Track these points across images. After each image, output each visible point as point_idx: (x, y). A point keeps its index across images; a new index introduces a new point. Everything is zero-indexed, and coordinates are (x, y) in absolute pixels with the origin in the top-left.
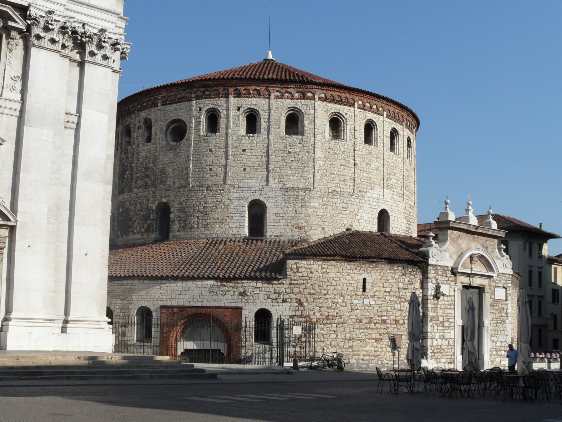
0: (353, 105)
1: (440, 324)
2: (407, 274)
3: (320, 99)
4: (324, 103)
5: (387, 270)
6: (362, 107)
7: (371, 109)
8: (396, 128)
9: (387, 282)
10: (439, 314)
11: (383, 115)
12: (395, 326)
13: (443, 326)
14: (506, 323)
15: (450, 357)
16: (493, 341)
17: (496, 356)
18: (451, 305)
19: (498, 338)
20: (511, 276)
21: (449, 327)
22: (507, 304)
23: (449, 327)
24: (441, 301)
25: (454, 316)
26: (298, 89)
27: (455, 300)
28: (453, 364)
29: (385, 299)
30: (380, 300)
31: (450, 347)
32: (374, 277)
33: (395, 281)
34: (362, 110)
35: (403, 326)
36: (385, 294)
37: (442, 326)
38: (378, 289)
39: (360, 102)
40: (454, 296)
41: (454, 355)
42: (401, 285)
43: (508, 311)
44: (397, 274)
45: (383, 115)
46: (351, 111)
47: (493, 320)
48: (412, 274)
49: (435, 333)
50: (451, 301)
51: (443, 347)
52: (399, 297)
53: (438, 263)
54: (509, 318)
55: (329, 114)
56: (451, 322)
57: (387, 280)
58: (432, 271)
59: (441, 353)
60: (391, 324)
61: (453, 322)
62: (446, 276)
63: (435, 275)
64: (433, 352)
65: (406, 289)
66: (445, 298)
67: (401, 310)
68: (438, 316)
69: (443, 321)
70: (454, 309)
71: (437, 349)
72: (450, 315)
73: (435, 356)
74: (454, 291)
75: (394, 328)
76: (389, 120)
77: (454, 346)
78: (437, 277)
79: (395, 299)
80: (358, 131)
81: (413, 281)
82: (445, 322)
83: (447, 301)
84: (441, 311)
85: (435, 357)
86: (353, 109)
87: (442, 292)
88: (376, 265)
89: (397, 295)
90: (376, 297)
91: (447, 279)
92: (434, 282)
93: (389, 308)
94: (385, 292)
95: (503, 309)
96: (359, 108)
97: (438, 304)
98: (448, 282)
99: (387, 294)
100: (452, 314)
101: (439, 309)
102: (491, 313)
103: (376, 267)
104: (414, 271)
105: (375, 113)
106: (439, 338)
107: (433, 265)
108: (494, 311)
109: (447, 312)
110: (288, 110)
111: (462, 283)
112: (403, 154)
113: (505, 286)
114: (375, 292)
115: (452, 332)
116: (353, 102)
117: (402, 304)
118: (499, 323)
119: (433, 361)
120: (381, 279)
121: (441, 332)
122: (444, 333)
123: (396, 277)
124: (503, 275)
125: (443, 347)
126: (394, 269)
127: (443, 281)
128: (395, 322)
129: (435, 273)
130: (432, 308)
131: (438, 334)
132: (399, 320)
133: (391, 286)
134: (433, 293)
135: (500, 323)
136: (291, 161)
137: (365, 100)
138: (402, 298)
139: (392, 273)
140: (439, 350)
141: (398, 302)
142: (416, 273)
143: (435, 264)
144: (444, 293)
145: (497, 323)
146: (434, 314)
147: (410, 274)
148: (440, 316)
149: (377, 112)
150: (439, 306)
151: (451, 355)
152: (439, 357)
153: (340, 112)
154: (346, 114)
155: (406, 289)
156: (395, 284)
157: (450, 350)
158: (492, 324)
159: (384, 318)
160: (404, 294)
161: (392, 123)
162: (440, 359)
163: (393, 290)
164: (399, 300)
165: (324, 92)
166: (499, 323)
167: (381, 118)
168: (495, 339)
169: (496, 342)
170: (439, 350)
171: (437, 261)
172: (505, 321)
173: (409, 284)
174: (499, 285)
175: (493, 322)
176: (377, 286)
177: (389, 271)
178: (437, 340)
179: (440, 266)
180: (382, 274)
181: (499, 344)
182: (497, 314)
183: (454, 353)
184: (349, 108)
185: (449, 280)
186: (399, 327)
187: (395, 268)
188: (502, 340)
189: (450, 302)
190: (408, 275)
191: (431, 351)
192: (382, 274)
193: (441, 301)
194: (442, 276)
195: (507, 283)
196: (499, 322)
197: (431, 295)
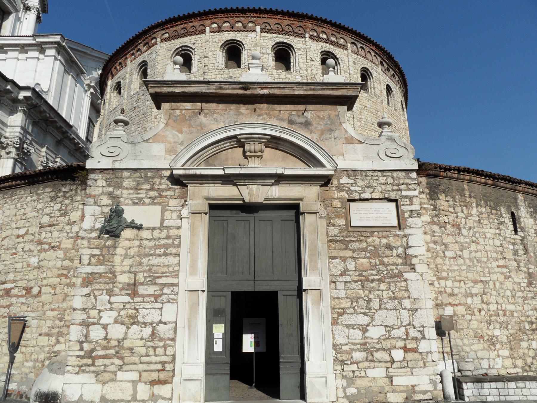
0: (203, 32)
1: (122, 289)
2: (59, 197)
3: (164, 40)
4: (168, 43)
5: (26, 198)
6: (217, 29)
7: (232, 29)
8: (285, 41)
9: (24, 217)
10: (118, 269)
11: (255, 31)
12: (23, 300)
13: (134, 294)
14: (406, 280)
15: (159, 367)
16: (348, 326)
17: (366, 364)
18: (166, 246)
19: (372, 317)
20: (414, 175)
21: (156, 297)
22: (406, 236)
23: (156, 297)
24: (127, 239)
25: (178, 271)
26: (145, 42)
27: (180, 237)
28: (169, 386)
29: (16, 249)
30: (8, 252)
31: (161, 344)
32: (7, 213)
33: (36, 214)
34: (217, 33)
35: (37, 300)
36: (18, 240)
37: (128, 295)
38: (9, 232)
39: (215, 26)
40: (179, 228)
41: (173, 360)
42: (46, 220)
43: (410, 252)
44: (41, 201)
45: (255, 31)
46: (201, 39)
47: (343, 274)
48: (68, 195)
49: (100, 311)
50: (168, 237)
51: (127, 344)
52: (40, 243)
53: (117, 166)
54: (418, 268)
55: (172, 52)
56: (164, 285)
57: (25, 214)
58: (101, 182)
59: (122, 358)
60: (18, 296)
61: (173, 285)
62: (152, 189)
63: (111, 189)
64: (89, 354)
65: (54, 225)
66: (145, 234)
67: (39, 268)
68: (113, 273)
69: (134, 284)
70: (179, 255)
71: (105, 348)
72: (165, 269)
73: (93, 365)
74: (180, 217)
75: (22, 303)
76: (269, 35)
77: (174, 340)
78: (118, 192)
79: (32, 248)
80: (210, 57)
81: (69, 208)
82: (142, 284)
83: (150, 240)
84: (127, 262)
85: (92, 368)
86: (203, 35)
87: (133, 220)
88: (13, 192)
89: (36, 239)
90: (3, 247)
91: (152, 194)
92: (106, 201)
93: (19, 266)
94: (18, 236)
95: (389, 247)
96: (211, 32)
97: (115, 247)
98: (159, 200)
99: (21, 239)
100: (168, 266)
101: (117, 259)
102: (334, 258)
103: (12, 196)
104: (71, 190)
105: (240, 31)
106: (116, 322)
107: (102, 171)
108: (349, 254)
109: (150, 262)
110: (139, 67)
111: (208, 199)
112: (307, 70)
113: (393, 196)
114: (5, 238)
115: (167, 307)
116: (204, 28)
117: (43, 255)
118: (373, 281)
119: (87, 378)
120: (16, 215)
121: (124, 308)
122: (137, 310)
123: (40, 206)
124: (380, 174)
125: (127, 344)
126: (37, 194)
127: (141, 199)
128: (24, 292)
129: (109, 185)
130: (93, 256)
131: (114, 314)
132: (31, 288)
133: (27, 225)
134: (98, 226)
135: (381, 281)
136: (134, 117)
137: (220, 21)
138: (44, 243)
139: (34, 201)
140: (112, 352)
141: (36, 252)
142: (76, 192)
143: (110, 167)
144: (138, 222)
145: (363, 280)
146: (101, 269)
147: (64, 196)
148: (123, 272)
149: (245, 29)
150: (119, 251)
151: (163, 363)
152: (112, 368)
153: (186, 44)
154: (194, 44)
155: (54, 225)
156: (35, 219)
157: (160, 351)
158: (340, 286)
159: (8, 286)
160: (49, 235)
161: (276, 37)
162: (115, 373)
163: (30, 232)
164: (39, 248)
165: (167, 31)
166: (373, 281)
167: (253, 34)
168: (363, 320)
169: (364, 329)
170: (112, 352)
171: (114, 161)
172: (400, 275)
173: (62, 215)
174: (366, 195)
175: (348, 279)
176: (8, 227)
177: (29, 199)
178: (105, 327)
179: (127, 170)
180: (19, 205)
181: (375, 333)
182: (365, 261)
183: (174, 356)
184: (199, 36)
185: (161, 196)
186: (31, 300)
187: (39, 192)
188: (391, 320)
189: (163, 242)
190: (60, 200)
191: (82, 353)
192: (19, 205)
193: (127, 239)
194: (137, 189)
195: (401, 190)
196: (371, 277)
197: (92, 230)
